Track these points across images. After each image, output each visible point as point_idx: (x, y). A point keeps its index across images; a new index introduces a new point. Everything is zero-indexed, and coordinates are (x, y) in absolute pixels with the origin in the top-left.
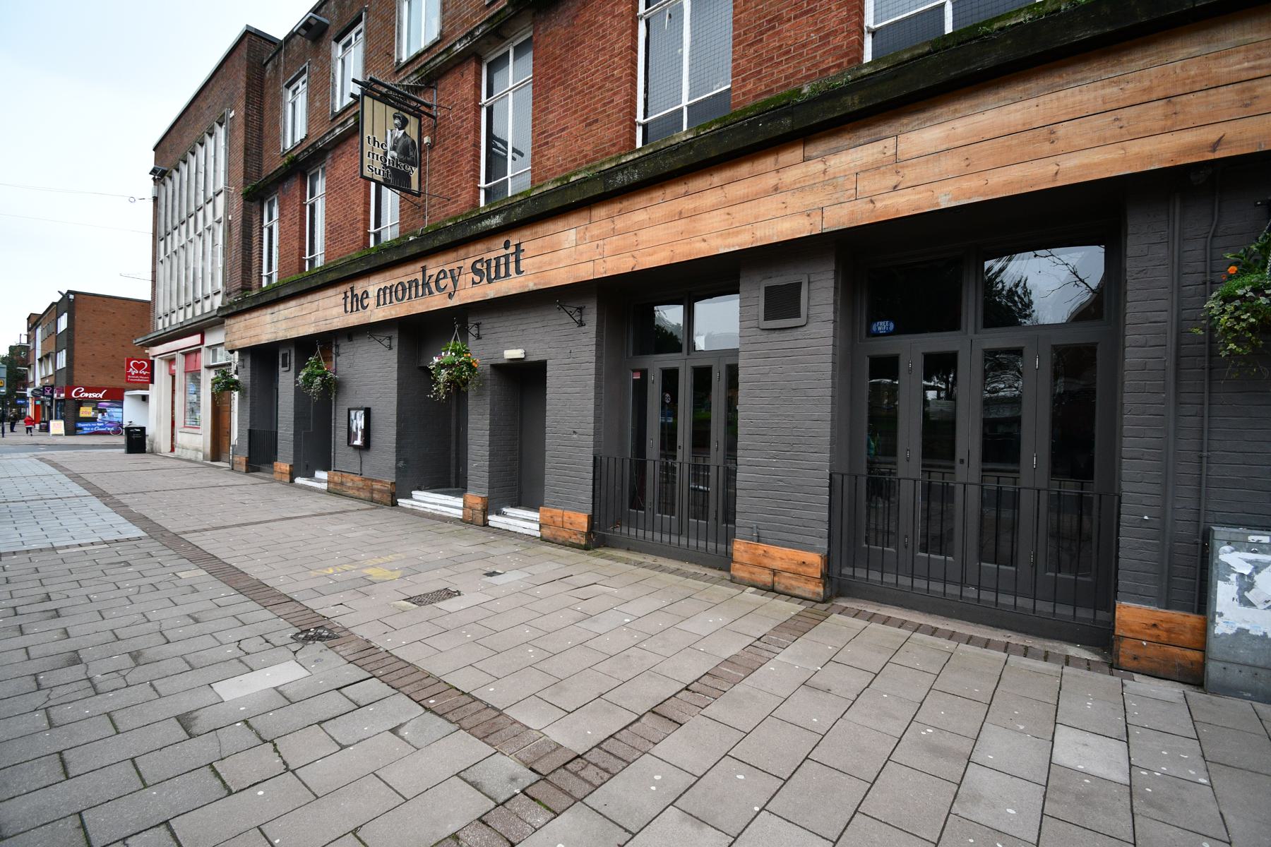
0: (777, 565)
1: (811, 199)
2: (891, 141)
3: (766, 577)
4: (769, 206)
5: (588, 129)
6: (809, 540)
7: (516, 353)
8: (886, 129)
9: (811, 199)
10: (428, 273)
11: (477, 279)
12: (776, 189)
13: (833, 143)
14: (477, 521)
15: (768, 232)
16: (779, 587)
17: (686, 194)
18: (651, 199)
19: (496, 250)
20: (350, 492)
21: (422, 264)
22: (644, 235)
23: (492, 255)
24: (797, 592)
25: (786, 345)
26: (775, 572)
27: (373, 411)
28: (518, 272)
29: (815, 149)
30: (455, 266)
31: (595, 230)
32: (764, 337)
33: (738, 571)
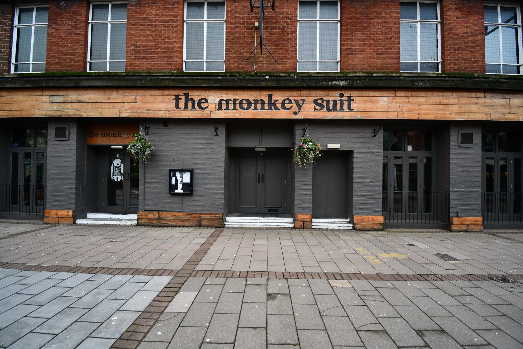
0: (468, 223)
1: (487, 110)
2: (508, 100)
3: (464, 228)
4: (475, 108)
5: (378, 56)
6: (475, 213)
7: (337, 146)
8: (507, 96)
9: (487, 110)
10: (273, 98)
11: (318, 108)
12: (476, 104)
13: (493, 95)
14: (306, 227)
15: (474, 116)
16: (469, 230)
17: (442, 96)
18: (427, 94)
19: (334, 96)
20: (172, 223)
21: (270, 93)
22: (423, 107)
23: (330, 98)
24: (475, 230)
25: (467, 152)
26: (467, 225)
27: (195, 171)
28: (350, 108)
29: (488, 95)
30: (299, 98)
31: (398, 100)
32: (459, 149)
33: (454, 228)
